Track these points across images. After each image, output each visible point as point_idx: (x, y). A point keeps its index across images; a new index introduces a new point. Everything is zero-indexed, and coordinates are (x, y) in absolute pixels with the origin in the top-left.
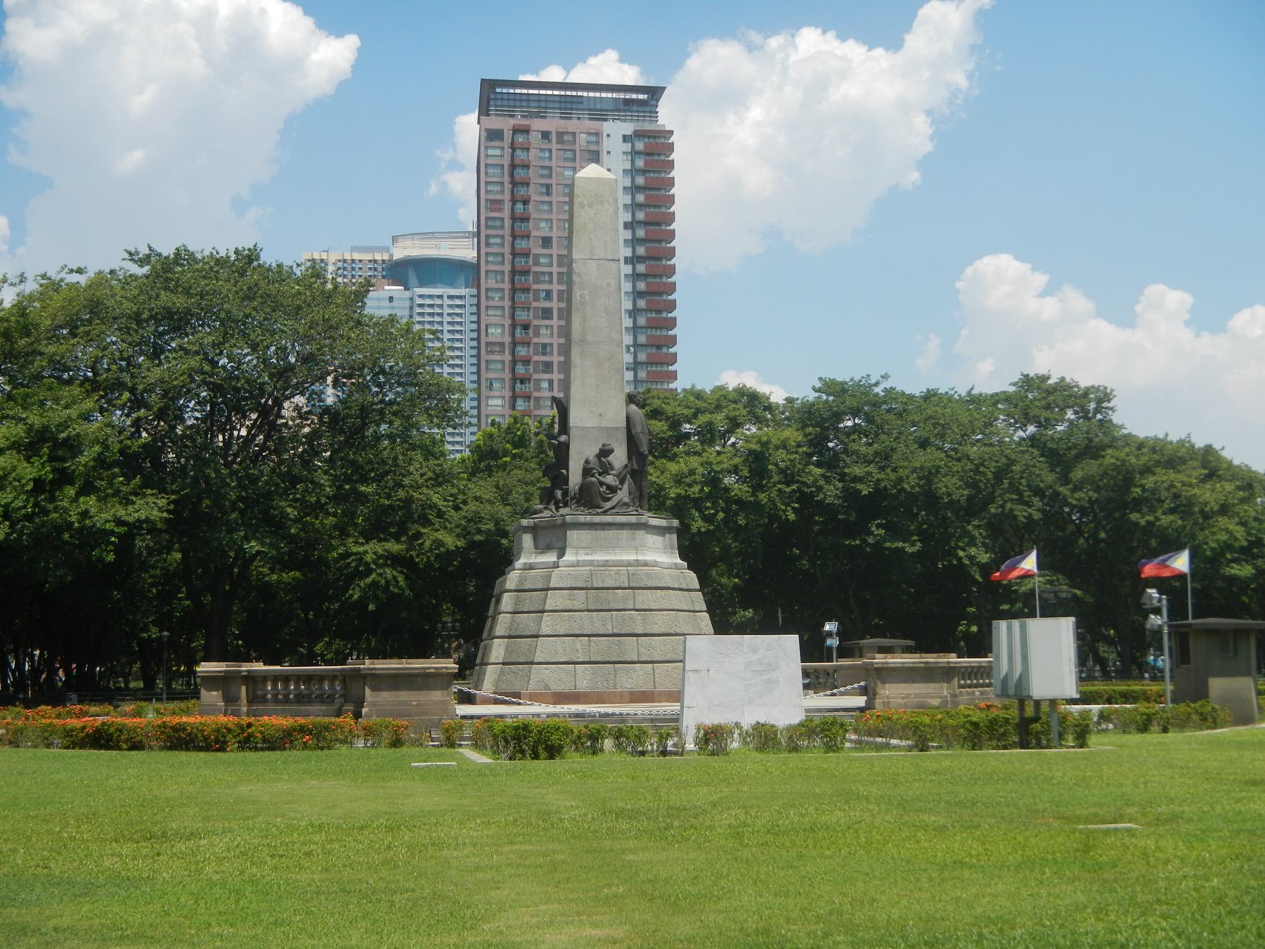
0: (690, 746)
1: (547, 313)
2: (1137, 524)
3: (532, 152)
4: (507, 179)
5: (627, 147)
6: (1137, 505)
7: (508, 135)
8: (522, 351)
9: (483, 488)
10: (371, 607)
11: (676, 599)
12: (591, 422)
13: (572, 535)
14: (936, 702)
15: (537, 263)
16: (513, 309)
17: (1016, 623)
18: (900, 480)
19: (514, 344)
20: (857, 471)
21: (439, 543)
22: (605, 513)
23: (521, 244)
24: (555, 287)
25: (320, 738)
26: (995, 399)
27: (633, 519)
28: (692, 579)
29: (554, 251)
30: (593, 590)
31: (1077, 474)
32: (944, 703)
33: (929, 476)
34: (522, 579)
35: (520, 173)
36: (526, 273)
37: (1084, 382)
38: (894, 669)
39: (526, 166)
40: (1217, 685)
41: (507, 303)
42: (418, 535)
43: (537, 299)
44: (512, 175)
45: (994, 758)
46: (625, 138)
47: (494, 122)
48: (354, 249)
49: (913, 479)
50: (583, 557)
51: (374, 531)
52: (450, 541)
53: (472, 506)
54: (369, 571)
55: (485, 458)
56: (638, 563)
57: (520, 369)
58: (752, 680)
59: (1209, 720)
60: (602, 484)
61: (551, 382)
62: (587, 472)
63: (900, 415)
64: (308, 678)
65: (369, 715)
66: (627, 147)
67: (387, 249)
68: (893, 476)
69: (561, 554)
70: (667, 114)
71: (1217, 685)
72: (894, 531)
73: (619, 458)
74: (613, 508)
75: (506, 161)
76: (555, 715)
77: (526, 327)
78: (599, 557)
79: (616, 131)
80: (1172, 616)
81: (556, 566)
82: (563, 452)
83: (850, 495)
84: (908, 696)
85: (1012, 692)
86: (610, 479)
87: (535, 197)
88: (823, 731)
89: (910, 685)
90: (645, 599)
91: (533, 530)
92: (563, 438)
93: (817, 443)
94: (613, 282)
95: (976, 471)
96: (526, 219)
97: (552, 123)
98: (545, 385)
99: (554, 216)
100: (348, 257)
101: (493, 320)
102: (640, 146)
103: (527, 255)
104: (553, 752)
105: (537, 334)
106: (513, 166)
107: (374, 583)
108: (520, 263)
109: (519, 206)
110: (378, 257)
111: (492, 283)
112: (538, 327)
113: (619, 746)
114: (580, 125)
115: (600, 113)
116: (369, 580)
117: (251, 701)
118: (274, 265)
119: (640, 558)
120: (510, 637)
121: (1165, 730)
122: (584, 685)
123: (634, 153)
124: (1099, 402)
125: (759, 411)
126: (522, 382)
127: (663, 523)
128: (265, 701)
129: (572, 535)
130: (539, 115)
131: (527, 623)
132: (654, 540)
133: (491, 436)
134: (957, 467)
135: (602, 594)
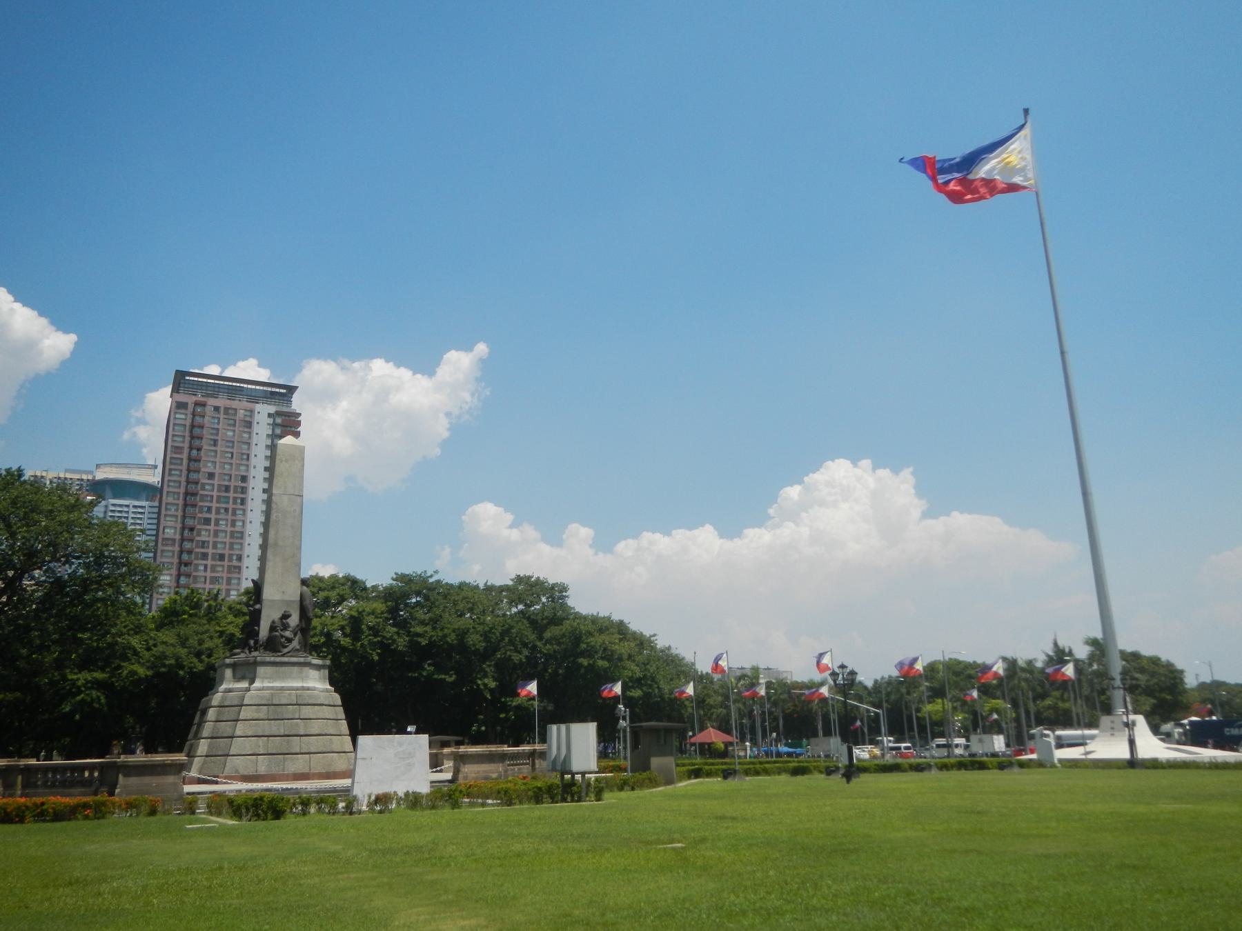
0: (364, 808)
1: (207, 521)
2: (581, 665)
3: (207, 418)
4: (187, 434)
5: (271, 421)
6: (583, 654)
7: (191, 407)
8: (187, 545)
9: (168, 636)
10: (77, 717)
11: (327, 712)
12: (277, 597)
13: (261, 670)
14: (494, 776)
15: (203, 488)
16: (184, 517)
17: (563, 727)
18: (445, 636)
19: (183, 540)
20: (419, 629)
21: (133, 673)
23: (193, 476)
24: (214, 505)
25: (100, 812)
26: (502, 589)
27: (302, 660)
28: (337, 699)
29: (216, 482)
30: (274, 707)
31: (547, 635)
32: (500, 776)
33: (462, 634)
34: (223, 699)
35: (197, 431)
36: (195, 494)
37: (551, 581)
39: (202, 427)
40: (655, 762)
41: (180, 513)
42: (119, 667)
43: (201, 512)
44: (191, 431)
45: (547, 809)
46: (270, 415)
47: (182, 398)
48: (67, 471)
49: (453, 636)
50: (266, 684)
51: (84, 665)
52: (142, 671)
53: (161, 648)
54: (80, 692)
55: (170, 616)
56: (303, 688)
57: (185, 557)
58: (397, 763)
59: (653, 783)
60: (282, 636)
61: (206, 566)
62: (273, 628)
63: (445, 596)
64: (74, 768)
65: (119, 794)
66: (271, 421)
67: (90, 472)
68: (440, 634)
69: (252, 681)
70: (297, 403)
71: (655, 762)
72: (440, 668)
73: (294, 620)
75: (188, 423)
76: (251, 790)
77: (192, 529)
78: (277, 684)
79: (263, 411)
80: (632, 721)
81: (248, 690)
82: (256, 617)
83: (413, 645)
85: (559, 768)
86: (288, 634)
87: (205, 447)
88: (447, 796)
89: (482, 766)
90: (307, 711)
91: (234, 666)
92: (257, 606)
93: (393, 611)
94: (298, 510)
95: (490, 631)
96: (198, 460)
97: (222, 402)
98: (202, 568)
99: (217, 460)
100: (62, 475)
101: (169, 524)
102: (279, 420)
103: (197, 483)
104: (278, 814)
105: (199, 534)
106: (192, 426)
108: (192, 488)
109: (194, 452)
110: (85, 477)
111: (170, 500)
112: (200, 530)
113: (320, 810)
114: (241, 405)
115: (254, 398)
116: (79, 698)
117: (24, 787)
120: (212, 738)
121: (633, 789)
122: (262, 770)
123: (275, 425)
124: (561, 592)
125: (358, 592)
126: (186, 565)
128: (36, 786)
130: (212, 396)
131: (225, 728)
132: (314, 673)
133: (175, 601)
134: (480, 628)
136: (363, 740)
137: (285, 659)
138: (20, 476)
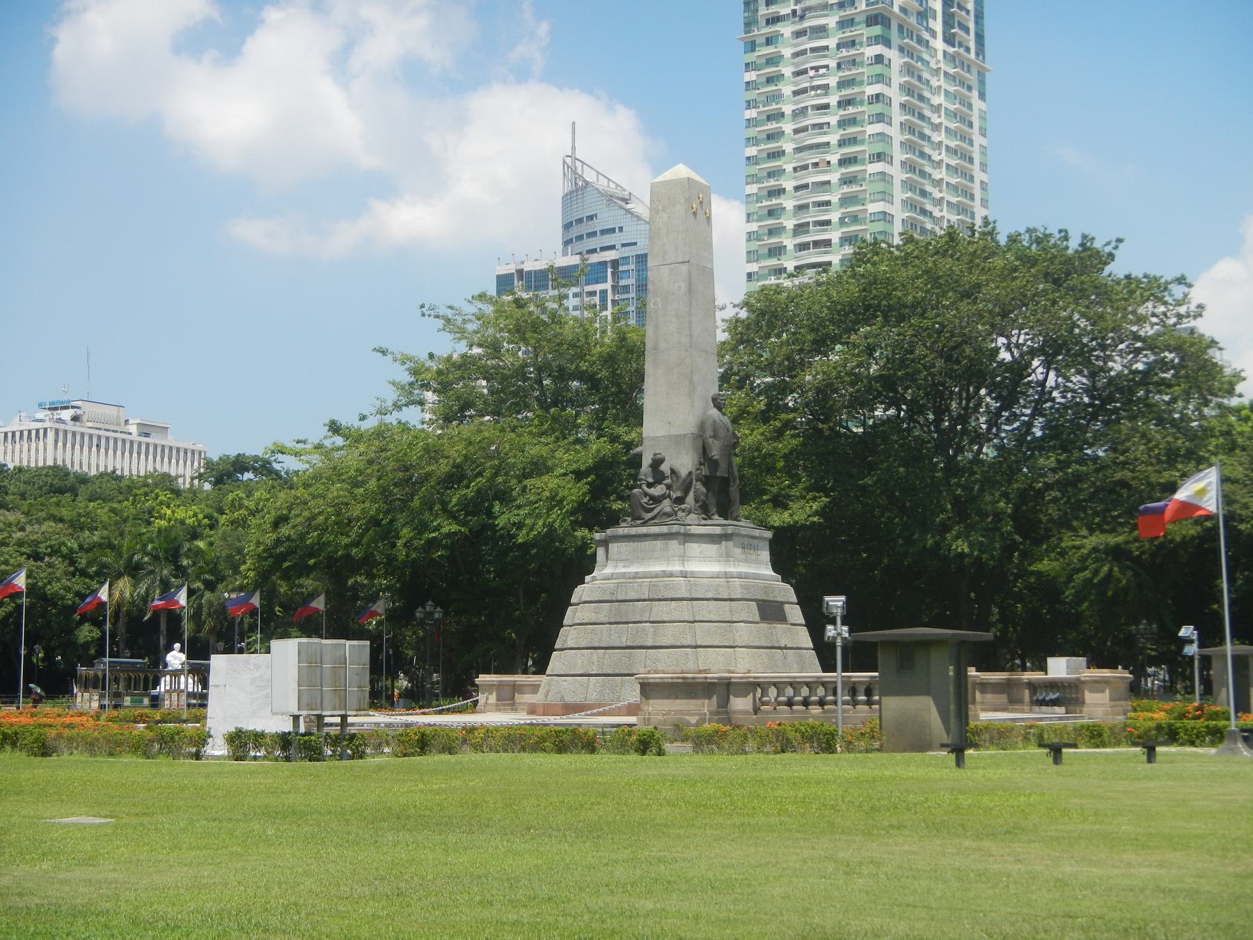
22: (644, 524)
27: (664, 529)
38: (657, 685)
60: (646, 494)
73: (684, 462)
74: (653, 518)
84: (668, 713)
86: (658, 491)
90: (661, 610)
94: (683, 285)
119: (670, 569)
127: (718, 530)
129: (614, 547)
136: (218, 662)
137: (644, 530)
138: (991, 233)
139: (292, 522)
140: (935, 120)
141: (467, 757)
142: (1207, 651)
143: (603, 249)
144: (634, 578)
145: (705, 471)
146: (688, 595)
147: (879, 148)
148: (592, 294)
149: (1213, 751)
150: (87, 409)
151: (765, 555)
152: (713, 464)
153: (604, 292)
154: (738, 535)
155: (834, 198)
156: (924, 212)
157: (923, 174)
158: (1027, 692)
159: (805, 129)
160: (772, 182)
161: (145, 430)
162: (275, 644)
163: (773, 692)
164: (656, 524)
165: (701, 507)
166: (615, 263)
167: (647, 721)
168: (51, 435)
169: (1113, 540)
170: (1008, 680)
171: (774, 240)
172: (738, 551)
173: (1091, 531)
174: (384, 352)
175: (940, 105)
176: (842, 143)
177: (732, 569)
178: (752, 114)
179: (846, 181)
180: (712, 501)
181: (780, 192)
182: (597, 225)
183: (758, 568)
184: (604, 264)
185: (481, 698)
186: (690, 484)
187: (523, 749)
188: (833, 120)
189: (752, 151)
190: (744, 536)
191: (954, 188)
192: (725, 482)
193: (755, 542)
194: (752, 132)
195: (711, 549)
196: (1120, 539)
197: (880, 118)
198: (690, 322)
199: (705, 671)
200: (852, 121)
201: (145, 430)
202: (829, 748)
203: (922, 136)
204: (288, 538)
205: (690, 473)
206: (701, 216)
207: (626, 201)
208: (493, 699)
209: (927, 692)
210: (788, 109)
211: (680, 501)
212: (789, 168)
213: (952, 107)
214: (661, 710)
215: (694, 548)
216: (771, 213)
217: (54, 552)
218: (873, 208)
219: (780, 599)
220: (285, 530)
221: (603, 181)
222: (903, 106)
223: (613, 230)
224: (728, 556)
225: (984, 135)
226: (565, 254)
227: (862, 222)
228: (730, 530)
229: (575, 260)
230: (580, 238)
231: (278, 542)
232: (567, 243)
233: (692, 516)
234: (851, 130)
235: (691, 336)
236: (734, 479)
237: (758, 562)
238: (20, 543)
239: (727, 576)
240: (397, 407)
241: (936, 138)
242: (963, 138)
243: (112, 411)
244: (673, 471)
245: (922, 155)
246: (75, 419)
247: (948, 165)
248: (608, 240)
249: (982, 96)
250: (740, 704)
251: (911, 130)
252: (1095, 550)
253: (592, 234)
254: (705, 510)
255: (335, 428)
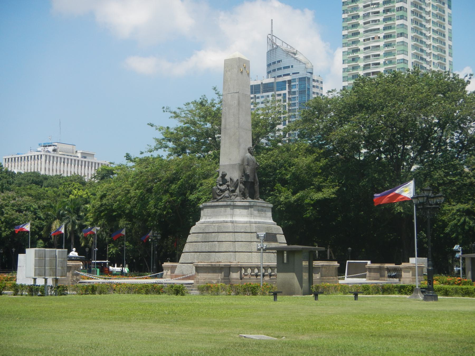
22: (217, 201)
27: (225, 203)
38: (201, 267)
60: (219, 189)
73: (235, 175)
74: (221, 199)
78: (212, 220)
90: (222, 237)
94: (236, 102)
107: (456, 225)
118: (209, 101)
127: (247, 204)
135: (207, 235)
139: (108, 197)
140: (428, 18)
141: (115, 296)
142: (465, 255)
143: (284, 75)
144: (213, 223)
145: (244, 179)
146: (236, 230)
147: (401, 31)
148: (279, 95)
149: (408, 296)
150: (59, 146)
151: (270, 214)
152: (247, 176)
153: (285, 94)
154: (256, 206)
155: (382, 53)
156: (422, 59)
157: (422, 42)
158: (386, 272)
159: (368, 23)
160: (354, 46)
161: (84, 155)
162: (27, 250)
163: (249, 271)
164: (222, 201)
165: (242, 194)
166: (290, 82)
167: (198, 282)
168: (43, 158)
169: (466, 206)
170: (380, 267)
171: (355, 72)
172: (256, 213)
173: (457, 203)
174: (152, 126)
175: (430, 11)
176: (385, 29)
177: (253, 220)
178: (345, 16)
179: (387, 45)
180: (247, 192)
181: (357, 50)
182: (282, 65)
183: (267, 219)
184: (285, 82)
185: (165, 272)
186: (238, 184)
187: (135, 293)
188: (381, 18)
189: (345, 32)
190: (259, 206)
191: (437, 48)
192: (253, 184)
193: (265, 209)
194: (346, 24)
195: (244, 211)
196: (469, 206)
197: (402, 17)
198: (239, 117)
199: (220, 262)
200: (389, 19)
201: (84, 155)
202: (254, 294)
203: (421, 25)
204: (105, 204)
205: (238, 180)
206: (245, 73)
207: (295, 54)
208: (169, 273)
209: (293, 272)
210: (361, 14)
211: (233, 191)
212: (361, 40)
213: (435, 12)
214: (203, 277)
215: (237, 211)
216: (354, 60)
217: (28, 209)
218: (399, 57)
219: (274, 233)
220: (104, 201)
221: (284, 47)
222: (413, 12)
223: (289, 67)
224: (251, 215)
225: (450, 24)
226: (268, 77)
227: (394, 63)
228: (252, 204)
229: (272, 80)
230: (274, 70)
231: (102, 205)
232: (269, 73)
233: (238, 198)
234: (389, 23)
235: (239, 123)
236: (257, 183)
237: (266, 217)
238: (13, 205)
239: (250, 223)
240: (157, 149)
241: (428, 26)
242: (440, 26)
243: (70, 147)
244: (231, 179)
245: (421, 33)
246: (54, 150)
247: (433, 38)
248: (287, 71)
249: (449, 7)
250: (235, 276)
251: (416, 23)
252: (458, 211)
253: (279, 69)
254: (244, 195)
255: (128, 157)
